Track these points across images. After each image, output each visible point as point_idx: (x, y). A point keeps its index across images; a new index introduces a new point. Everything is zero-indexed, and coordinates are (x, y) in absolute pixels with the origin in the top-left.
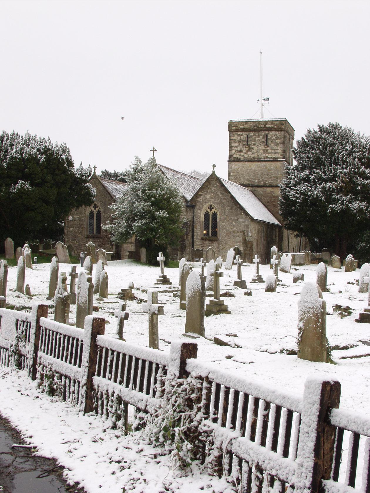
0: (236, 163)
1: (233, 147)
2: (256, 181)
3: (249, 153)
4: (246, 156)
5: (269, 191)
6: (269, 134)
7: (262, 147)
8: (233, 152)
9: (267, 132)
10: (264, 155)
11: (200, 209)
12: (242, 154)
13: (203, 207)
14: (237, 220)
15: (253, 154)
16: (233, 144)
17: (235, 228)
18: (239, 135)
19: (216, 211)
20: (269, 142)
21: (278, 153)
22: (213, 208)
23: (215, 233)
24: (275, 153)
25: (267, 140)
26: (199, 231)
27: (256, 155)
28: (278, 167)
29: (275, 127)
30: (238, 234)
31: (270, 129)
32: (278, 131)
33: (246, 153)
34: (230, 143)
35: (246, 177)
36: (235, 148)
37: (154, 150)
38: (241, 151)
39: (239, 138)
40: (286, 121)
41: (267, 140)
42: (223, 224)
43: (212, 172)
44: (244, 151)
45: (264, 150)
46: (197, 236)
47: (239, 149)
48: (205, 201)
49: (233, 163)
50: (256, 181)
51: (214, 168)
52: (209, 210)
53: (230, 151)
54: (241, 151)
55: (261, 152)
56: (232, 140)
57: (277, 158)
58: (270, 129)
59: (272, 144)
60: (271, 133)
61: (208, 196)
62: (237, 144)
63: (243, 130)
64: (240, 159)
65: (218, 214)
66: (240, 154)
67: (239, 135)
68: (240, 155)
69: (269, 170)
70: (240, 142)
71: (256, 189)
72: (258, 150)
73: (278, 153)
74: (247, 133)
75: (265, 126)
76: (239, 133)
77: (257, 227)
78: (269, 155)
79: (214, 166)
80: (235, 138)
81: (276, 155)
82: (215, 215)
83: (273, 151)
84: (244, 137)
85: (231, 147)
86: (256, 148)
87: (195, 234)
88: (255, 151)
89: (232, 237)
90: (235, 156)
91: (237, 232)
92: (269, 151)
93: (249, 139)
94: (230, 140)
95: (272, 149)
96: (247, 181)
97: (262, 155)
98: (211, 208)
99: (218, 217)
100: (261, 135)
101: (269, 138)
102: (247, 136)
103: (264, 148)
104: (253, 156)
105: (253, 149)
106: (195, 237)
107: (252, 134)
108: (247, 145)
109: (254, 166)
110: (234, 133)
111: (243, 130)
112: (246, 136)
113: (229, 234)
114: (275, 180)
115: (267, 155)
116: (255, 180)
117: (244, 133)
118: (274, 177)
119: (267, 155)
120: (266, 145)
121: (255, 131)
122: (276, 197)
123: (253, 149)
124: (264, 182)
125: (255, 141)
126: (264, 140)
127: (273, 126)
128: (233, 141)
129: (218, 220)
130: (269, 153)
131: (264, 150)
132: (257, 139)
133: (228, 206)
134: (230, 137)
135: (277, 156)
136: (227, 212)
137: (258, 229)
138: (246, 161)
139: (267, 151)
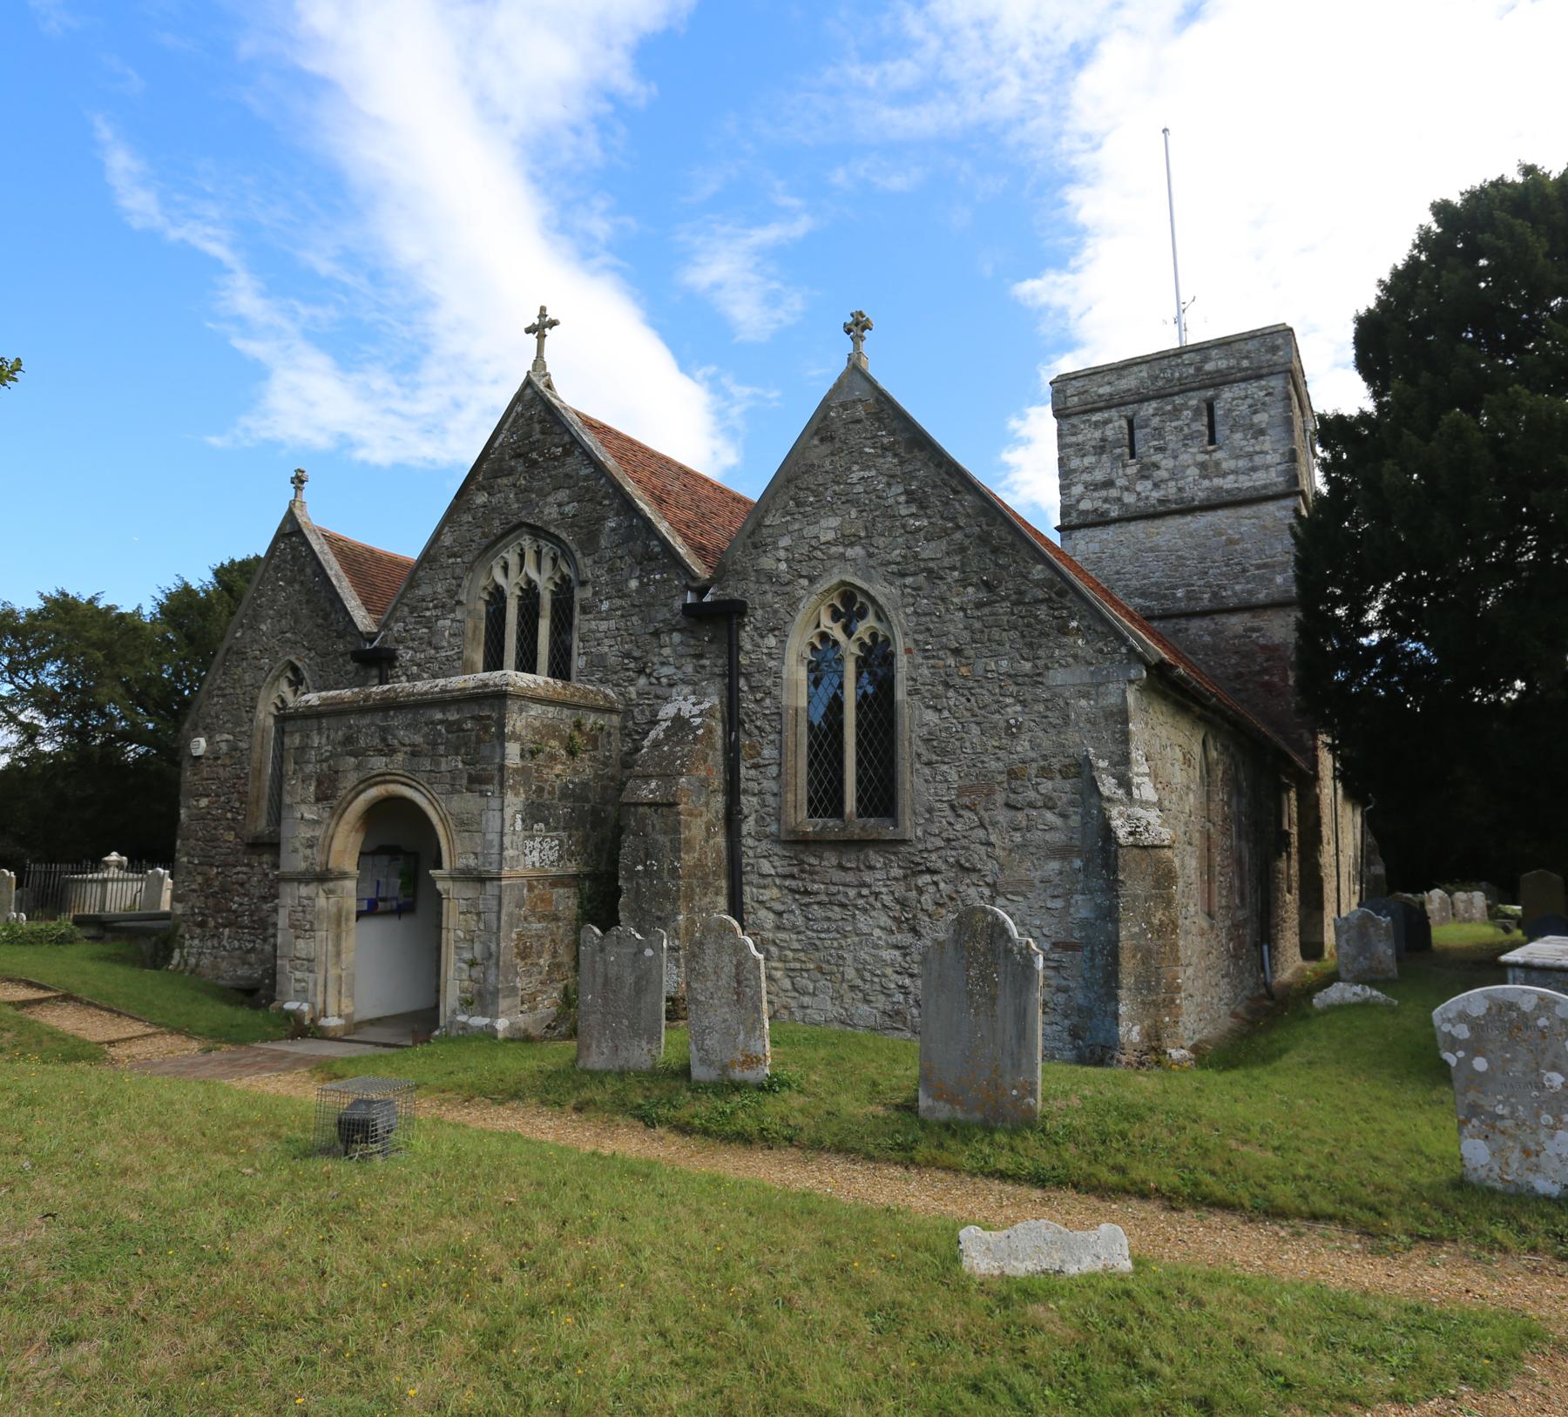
0: (1090, 532)
1: (1074, 471)
2: (1180, 593)
3: (1143, 487)
4: (1129, 498)
5: (1240, 629)
6: (1216, 397)
7: (1192, 455)
8: (1077, 490)
9: (1210, 393)
10: (1206, 483)
11: (779, 630)
12: (1114, 493)
13: (793, 604)
14: (1036, 678)
15: (1156, 486)
16: (1075, 463)
17: (1023, 746)
18: (1096, 425)
19: (881, 629)
20: (1222, 430)
21: (1267, 467)
22: (862, 614)
23: (881, 795)
24: (1254, 469)
25: (1211, 426)
26: (780, 782)
27: (1171, 490)
28: (1269, 522)
29: (1245, 363)
30: (1047, 786)
31: (1222, 380)
32: (1259, 377)
33: (1127, 489)
34: (1060, 459)
35: (1134, 583)
36: (1086, 477)
37: (541, 327)
38: (1109, 484)
39: (1098, 434)
40: (1289, 331)
41: (1211, 426)
42: (931, 717)
43: (841, 365)
44: (1121, 482)
45: (1202, 466)
46: (760, 821)
47: (1099, 476)
48: (809, 563)
49: (1078, 534)
50: (1180, 593)
51: (857, 339)
52: (837, 633)
53: (1064, 489)
54: (1109, 484)
55: (1193, 472)
56: (1070, 446)
57: (1265, 487)
58: (1222, 380)
59: (1238, 436)
60: (1227, 394)
61: (828, 528)
62: (1088, 460)
63: (1110, 403)
64: (1107, 512)
65: (900, 645)
66: (1104, 493)
67: (1096, 425)
68: (1106, 500)
69: (1231, 542)
70: (1100, 449)
71: (1183, 623)
72: (1182, 467)
73: (1267, 467)
74: (1128, 410)
75: (1198, 369)
76: (1096, 417)
77: (1197, 749)
78: (1228, 483)
79: (858, 326)
80: (1080, 438)
81: (1255, 476)
82: (877, 659)
83: (1241, 463)
84: (1116, 426)
85: (1065, 472)
86: (1168, 463)
87: (748, 803)
88: (1163, 474)
89: (1003, 816)
90: (1085, 505)
91: (1045, 772)
92: (1225, 465)
93: (1139, 434)
94: (1061, 447)
95: (1238, 457)
96: (1143, 595)
97: (1197, 487)
98: (850, 605)
99: (902, 662)
100: (1185, 406)
101: (1219, 412)
102: (1130, 423)
103: (1201, 458)
104: (1155, 494)
105: (1156, 466)
106: (749, 826)
107: (1149, 408)
108: (1132, 456)
109: (1167, 533)
110: (1075, 420)
111: (1110, 403)
112: (1124, 423)
113: (973, 795)
114: (1262, 578)
115: (1218, 482)
116: (1176, 587)
117: (1114, 413)
118: (1258, 567)
119: (1218, 482)
120: (1212, 441)
121: (1160, 396)
122: (1271, 651)
123: (1156, 466)
124: (1215, 595)
125: (1161, 437)
126: (1201, 426)
127: (1233, 362)
128: (1070, 451)
129: (901, 694)
130: (1224, 475)
131: (1202, 466)
132: (1170, 426)
133: (964, 583)
134: (1060, 436)
135: (1260, 479)
136: (956, 626)
137: (1208, 769)
138: (1129, 520)
139: (1217, 464)
